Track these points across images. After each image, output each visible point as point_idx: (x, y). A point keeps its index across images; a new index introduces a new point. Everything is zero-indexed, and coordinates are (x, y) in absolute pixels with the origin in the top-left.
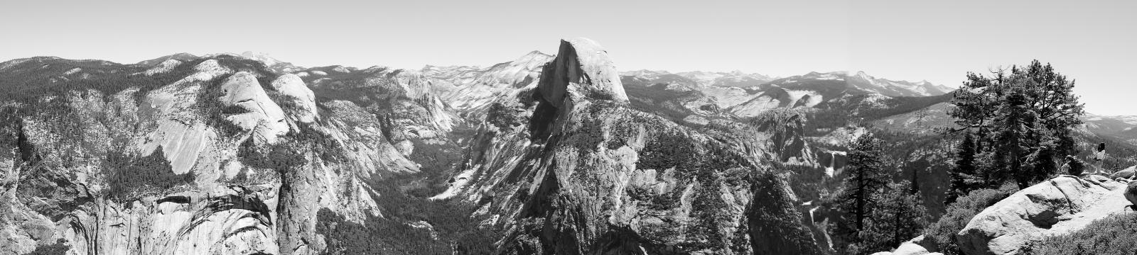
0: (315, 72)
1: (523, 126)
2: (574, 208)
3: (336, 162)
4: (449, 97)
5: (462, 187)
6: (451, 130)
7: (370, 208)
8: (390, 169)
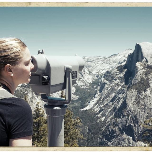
1: (118, 81)
2: (133, 116)
4: (92, 69)
5: (93, 105)
6: (92, 82)
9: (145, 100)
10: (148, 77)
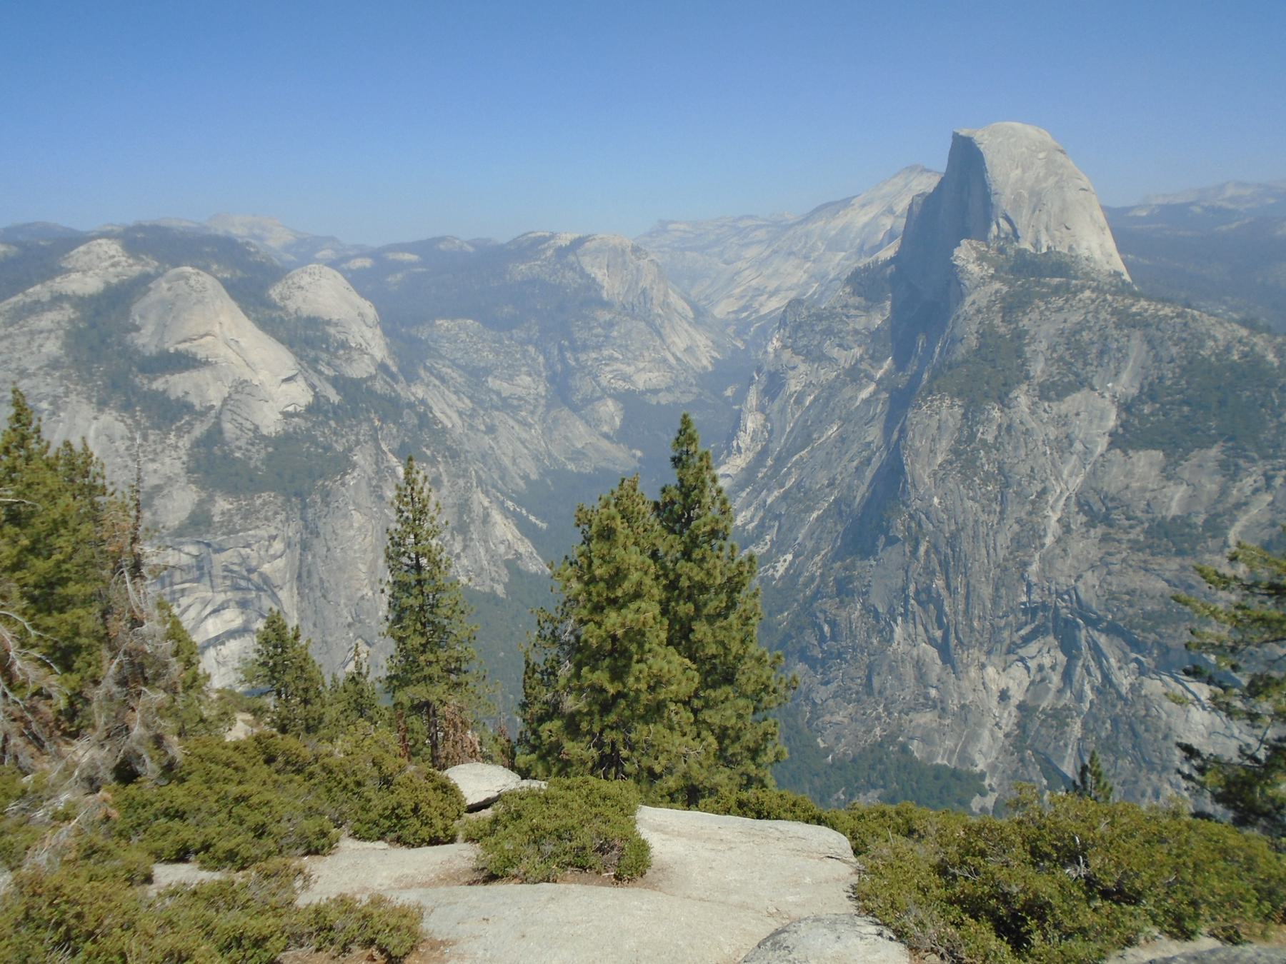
0: (391, 256)
3: (432, 461)
6: (710, 369)
7: (519, 556)
8: (571, 466)
9: (1005, 450)
10: (1021, 324)
